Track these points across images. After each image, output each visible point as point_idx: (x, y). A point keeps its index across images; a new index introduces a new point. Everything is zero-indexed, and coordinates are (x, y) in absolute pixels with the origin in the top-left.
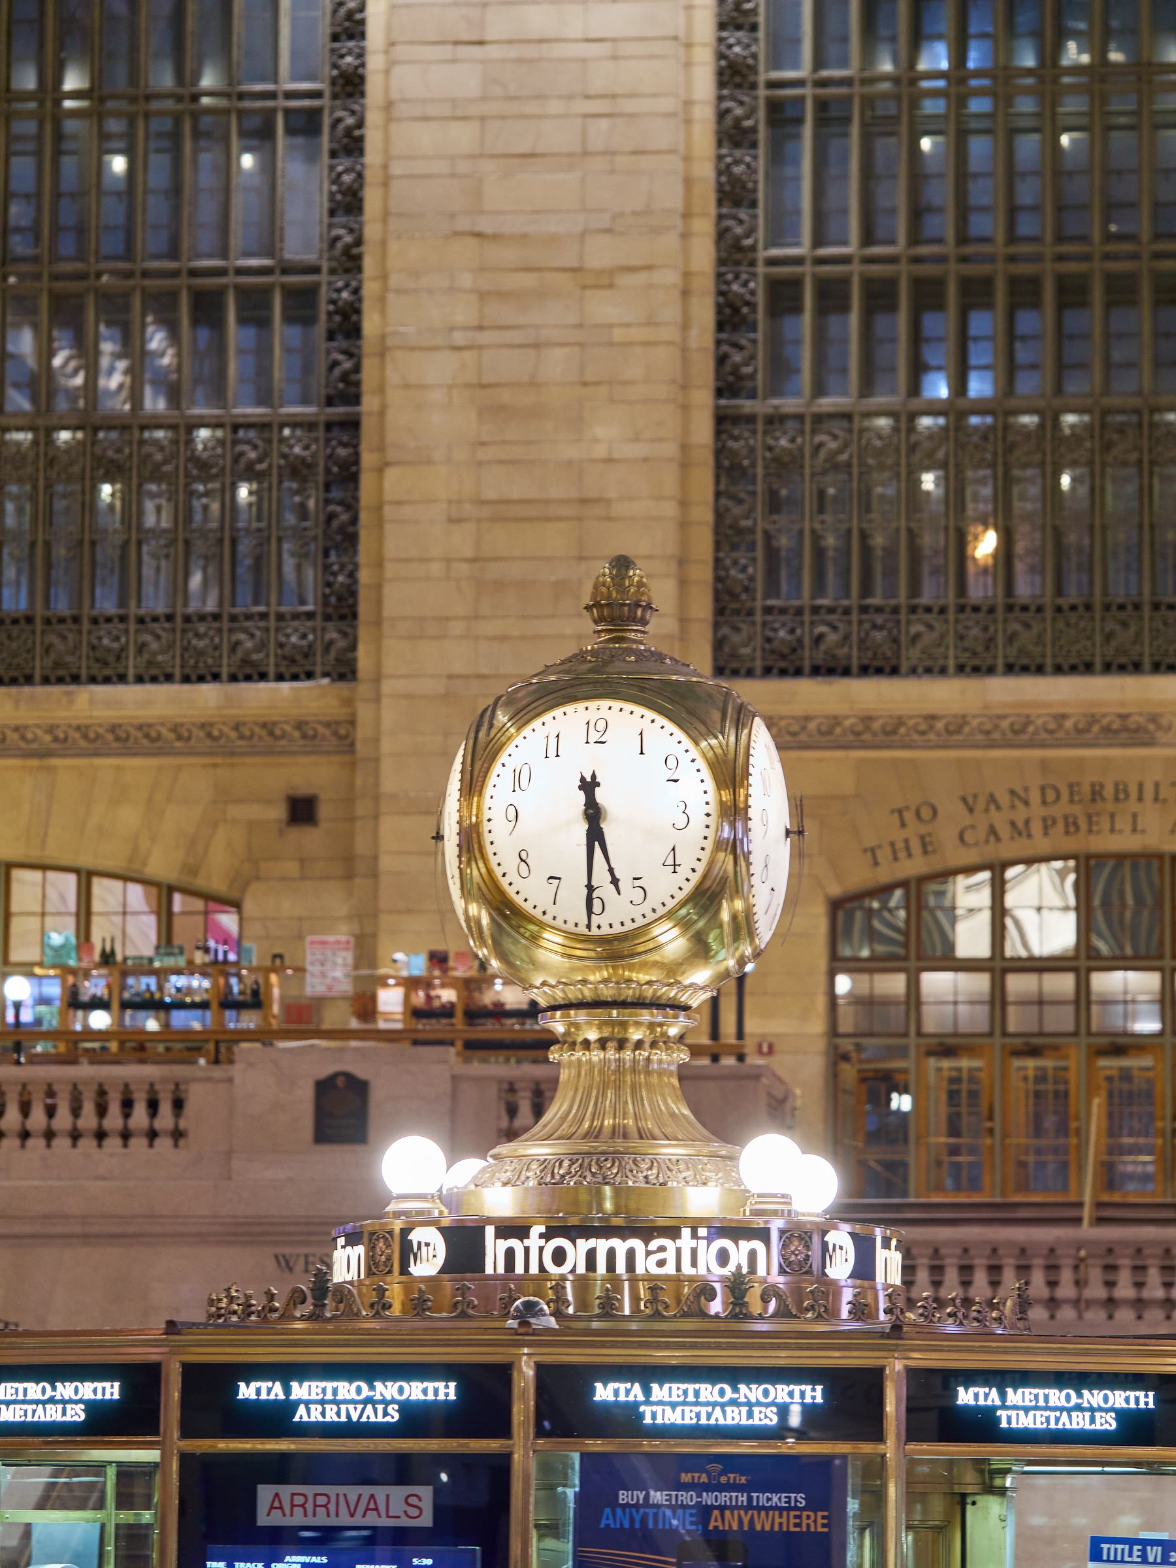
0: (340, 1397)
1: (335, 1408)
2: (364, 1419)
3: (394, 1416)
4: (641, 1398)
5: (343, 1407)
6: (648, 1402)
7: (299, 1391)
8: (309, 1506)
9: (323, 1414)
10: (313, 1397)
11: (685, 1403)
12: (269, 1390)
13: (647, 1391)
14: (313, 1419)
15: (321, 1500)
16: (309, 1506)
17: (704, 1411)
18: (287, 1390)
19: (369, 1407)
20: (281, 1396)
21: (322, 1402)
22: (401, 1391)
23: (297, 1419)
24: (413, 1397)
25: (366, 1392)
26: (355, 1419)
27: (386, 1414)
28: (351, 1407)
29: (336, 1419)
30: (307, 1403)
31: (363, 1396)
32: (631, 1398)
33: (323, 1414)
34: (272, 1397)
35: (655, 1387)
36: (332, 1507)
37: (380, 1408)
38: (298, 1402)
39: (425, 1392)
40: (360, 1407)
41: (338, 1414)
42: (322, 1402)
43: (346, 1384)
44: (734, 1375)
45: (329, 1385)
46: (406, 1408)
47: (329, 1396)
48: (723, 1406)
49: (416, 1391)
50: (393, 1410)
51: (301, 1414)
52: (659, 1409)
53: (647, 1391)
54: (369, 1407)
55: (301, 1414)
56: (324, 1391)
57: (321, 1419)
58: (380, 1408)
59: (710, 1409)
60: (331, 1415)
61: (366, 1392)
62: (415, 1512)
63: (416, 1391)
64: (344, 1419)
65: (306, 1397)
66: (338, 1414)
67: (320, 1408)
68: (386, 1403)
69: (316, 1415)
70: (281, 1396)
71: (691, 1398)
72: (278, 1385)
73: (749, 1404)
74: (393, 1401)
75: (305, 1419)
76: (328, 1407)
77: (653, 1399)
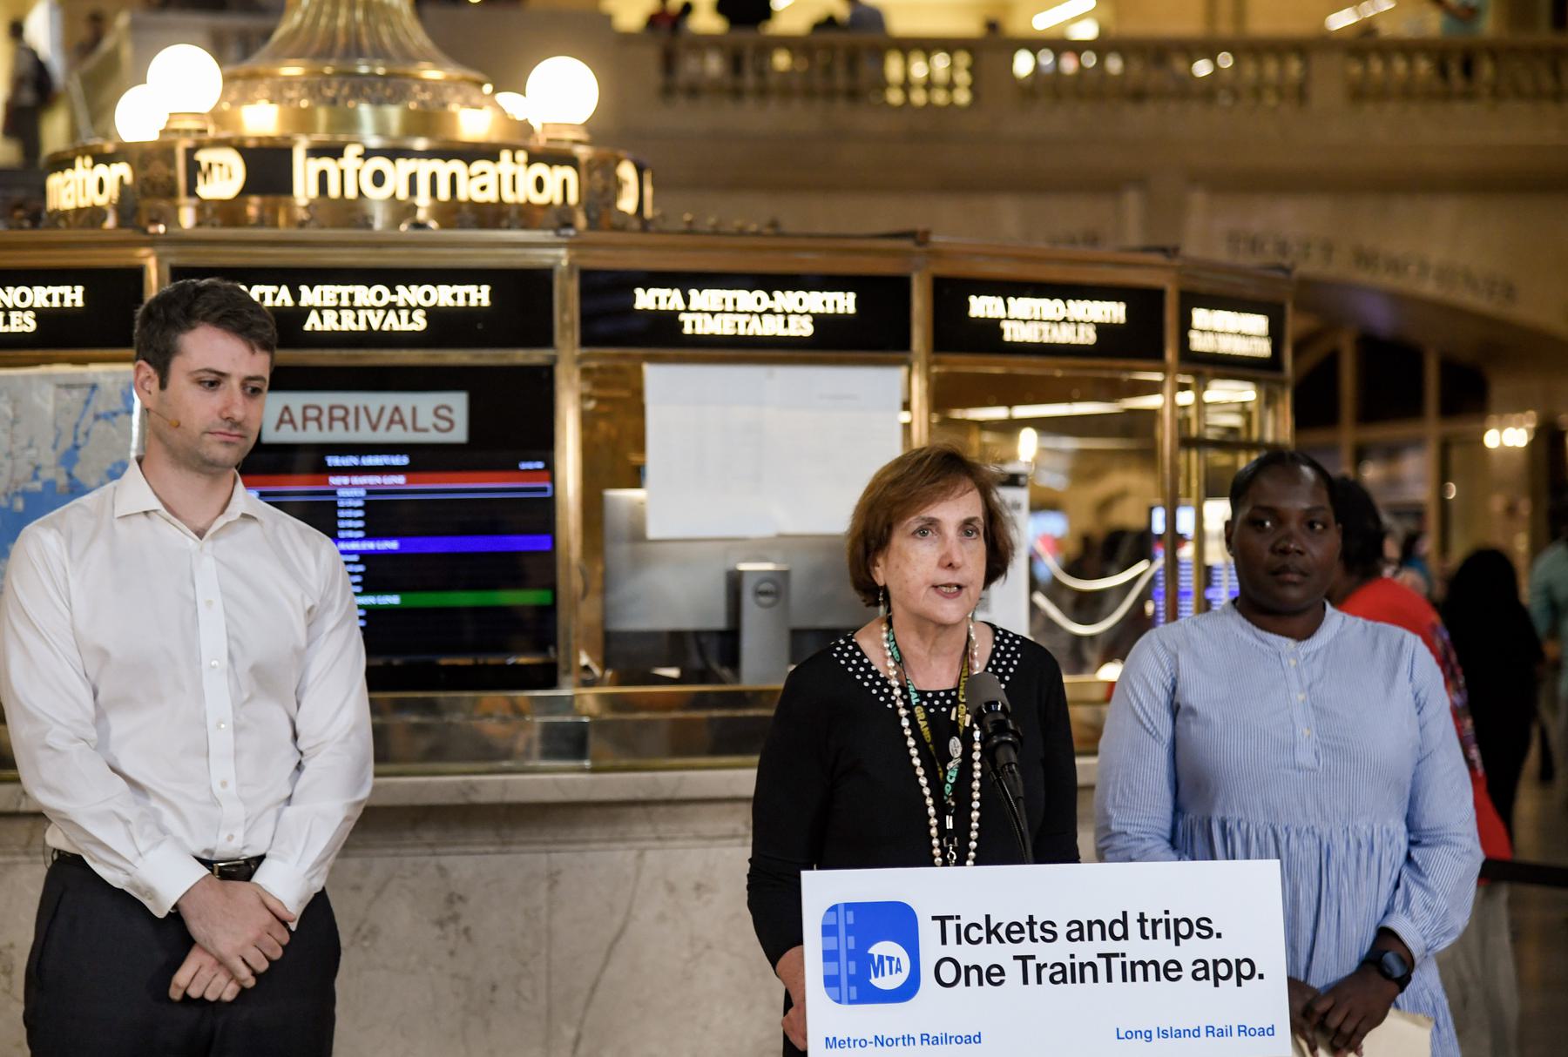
0: (357, 303)
1: (351, 314)
2: (386, 328)
3: (420, 323)
4: (681, 306)
5: (362, 313)
6: (687, 311)
7: (309, 296)
8: (325, 419)
9: (339, 321)
10: (327, 303)
11: (723, 312)
12: (275, 296)
13: (687, 300)
14: (327, 328)
15: (339, 413)
16: (325, 419)
17: (742, 319)
18: (296, 296)
19: (392, 313)
20: (289, 303)
21: (338, 308)
22: (427, 296)
23: (307, 327)
24: (441, 304)
25: (387, 297)
26: (375, 327)
27: (410, 320)
28: (370, 313)
29: (354, 327)
30: (320, 310)
31: (384, 302)
32: (671, 307)
33: (339, 321)
34: (278, 303)
35: (693, 293)
36: (351, 420)
37: (404, 314)
38: (311, 308)
39: (455, 297)
40: (381, 313)
41: (356, 321)
42: (338, 308)
43: (364, 288)
44: (770, 282)
45: (345, 290)
46: (433, 314)
47: (345, 302)
48: (760, 314)
49: (443, 295)
50: (419, 316)
51: (312, 323)
52: (698, 317)
53: (687, 300)
54: (392, 313)
55: (312, 323)
56: (339, 296)
57: (336, 327)
58: (404, 314)
59: (746, 317)
60: (348, 324)
61: (387, 297)
62: (444, 424)
63: (443, 295)
64: (362, 327)
65: (318, 304)
66: (356, 321)
67: (334, 314)
68: (411, 309)
69: (330, 323)
70: (289, 303)
71: (729, 307)
72: (284, 289)
73: (785, 313)
74: (419, 307)
75: (319, 327)
76: (344, 313)
77: (692, 307)
